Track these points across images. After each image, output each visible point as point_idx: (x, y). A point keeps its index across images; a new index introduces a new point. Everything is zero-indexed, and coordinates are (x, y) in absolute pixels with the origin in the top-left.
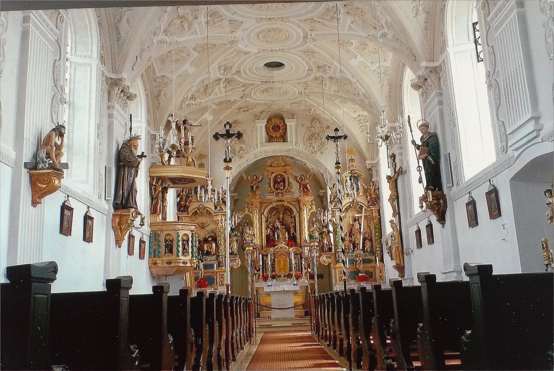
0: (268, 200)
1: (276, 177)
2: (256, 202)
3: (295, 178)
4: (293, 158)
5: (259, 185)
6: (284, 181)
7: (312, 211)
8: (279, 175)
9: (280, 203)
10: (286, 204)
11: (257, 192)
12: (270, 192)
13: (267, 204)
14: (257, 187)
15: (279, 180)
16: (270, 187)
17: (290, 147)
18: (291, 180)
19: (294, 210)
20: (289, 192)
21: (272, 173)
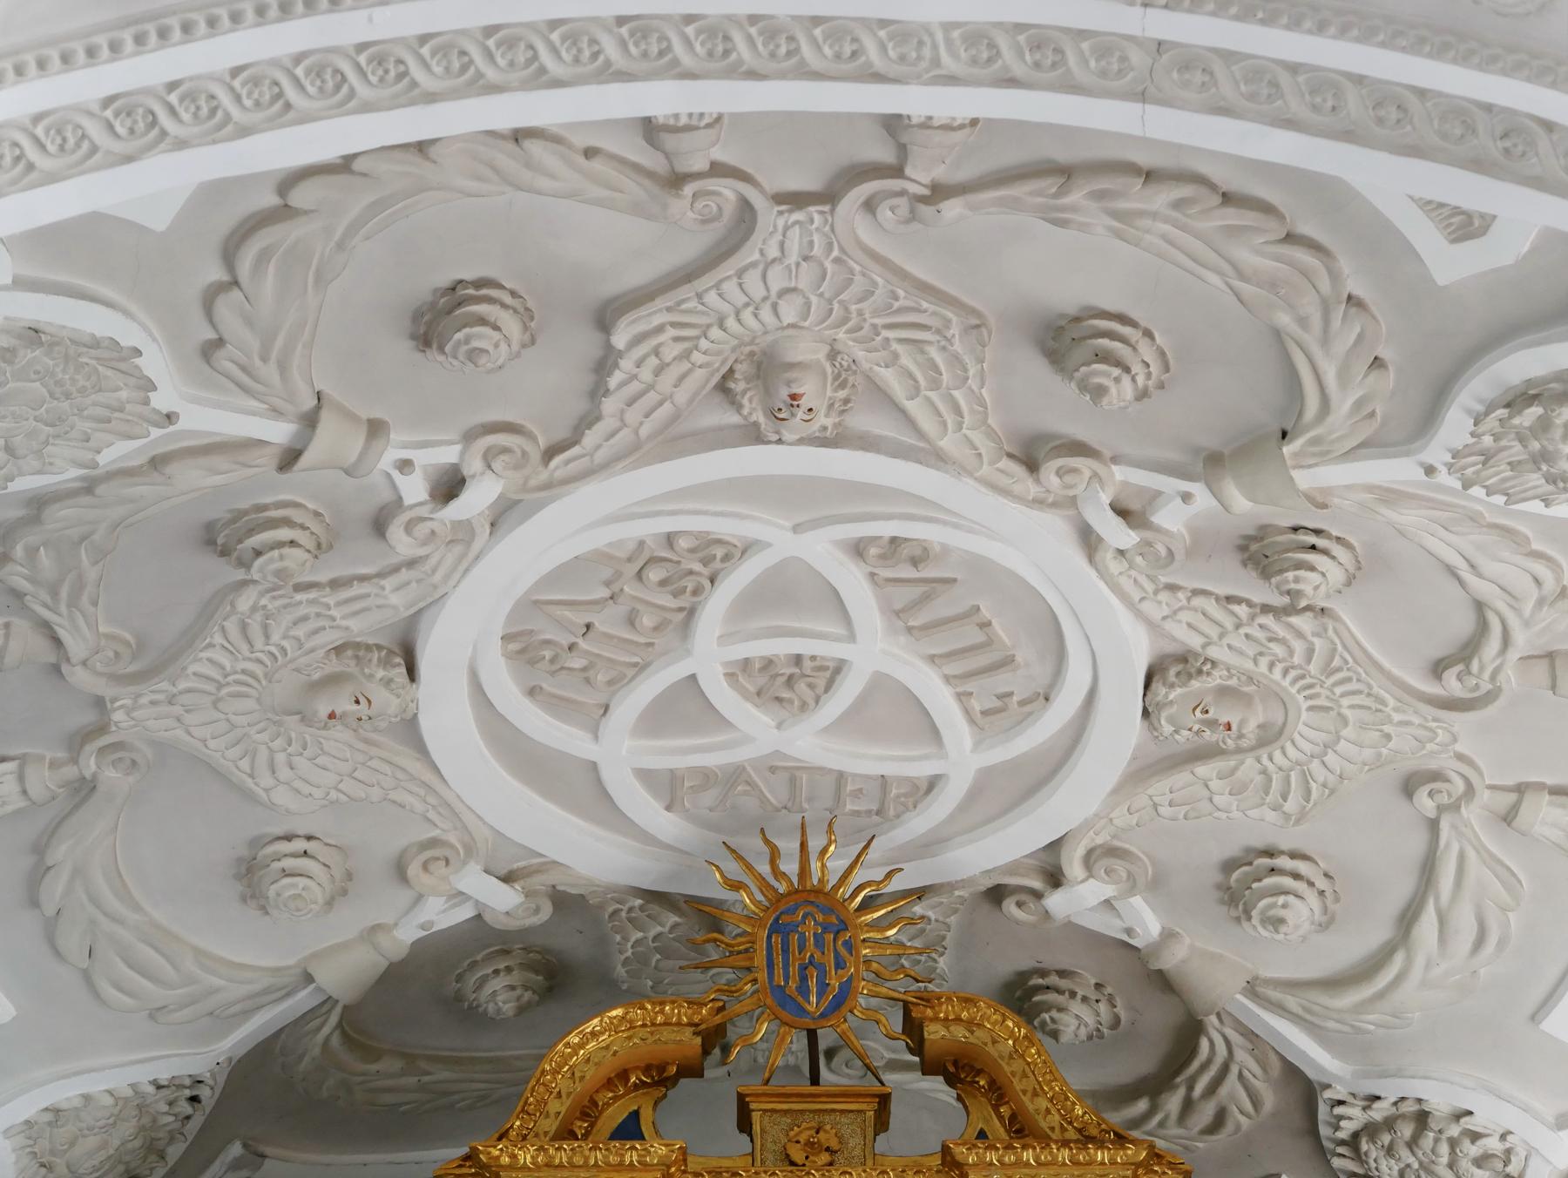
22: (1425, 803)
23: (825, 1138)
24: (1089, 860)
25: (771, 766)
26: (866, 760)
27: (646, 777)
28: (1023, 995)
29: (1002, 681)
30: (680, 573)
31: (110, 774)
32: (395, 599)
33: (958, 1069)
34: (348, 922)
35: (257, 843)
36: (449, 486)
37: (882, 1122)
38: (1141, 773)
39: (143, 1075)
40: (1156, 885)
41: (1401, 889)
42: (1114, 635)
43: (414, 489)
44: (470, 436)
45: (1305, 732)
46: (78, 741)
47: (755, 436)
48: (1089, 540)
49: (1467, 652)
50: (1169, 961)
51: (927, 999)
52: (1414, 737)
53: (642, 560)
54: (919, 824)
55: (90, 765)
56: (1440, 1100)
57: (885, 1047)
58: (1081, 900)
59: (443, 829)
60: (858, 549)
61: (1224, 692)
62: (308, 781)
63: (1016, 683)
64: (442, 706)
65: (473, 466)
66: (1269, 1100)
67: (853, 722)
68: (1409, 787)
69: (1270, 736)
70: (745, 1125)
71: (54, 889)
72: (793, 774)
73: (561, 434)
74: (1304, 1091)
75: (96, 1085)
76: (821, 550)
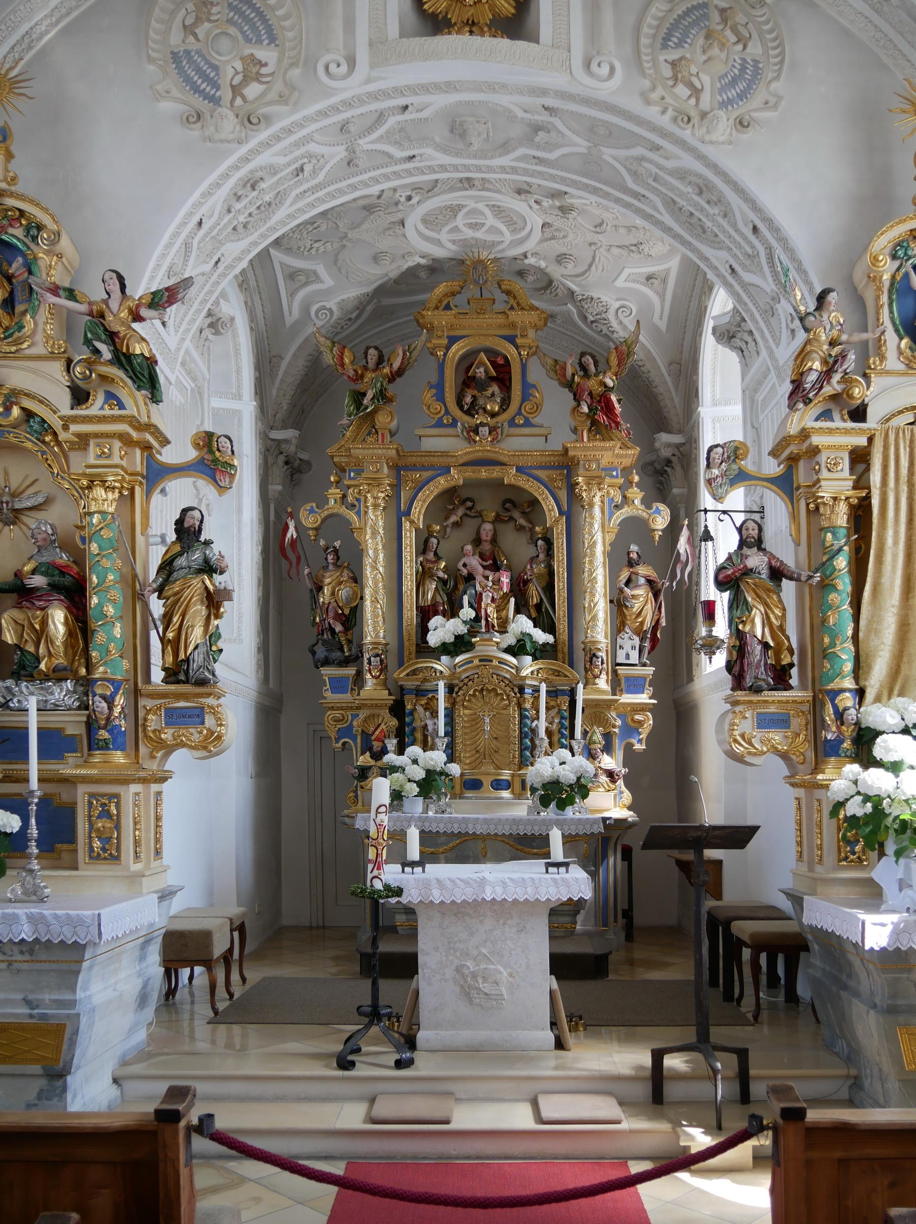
0: (430, 454)
1: (467, 362)
2: (376, 455)
3: (557, 369)
4: (547, 284)
5: (391, 390)
6: (502, 374)
7: (625, 512)
8: (489, 352)
9: (484, 473)
10: (510, 476)
11: (382, 419)
12: (439, 424)
13: (427, 474)
14: (382, 396)
15: (480, 372)
16: (440, 397)
17: (557, 80)
18: (537, 373)
19: (549, 505)
20: (528, 424)
22: (593, 247)
25: (472, 238)
26: (490, 238)
27: (449, 241)
28: (521, 273)
29: (515, 226)
30: (454, 210)
31: (348, 244)
32: (400, 216)
34: (394, 266)
35: (377, 254)
36: (409, 198)
38: (541, 241)
39: (358, 293)
40: (545, 259)
41: (589, 260)
42: (535, 220)
43: (403, 199)
44: (413, 190)
45: (571, 236)
46: (342, 239)
47: (467, 189)
48: (531, 208)
49: (601, 225)
50: (548, 270)
51: (502, 281)
52: (591, 237)
53: (446, 208)
55: (344, 242)
56: (595, 296)
58: (531, 261)
59: (411, 250)
60: (487, 206)
61: (556, 230)
62: (386, 243)
63: (518, 226)
64: (410, 230)
65: (413, 195)
66: (565, 292)
67: (488, 231)
68: (590, 244)
69: (564, 237)
70: (469, 303)
71: (339, 263)
72: (476, 239)
73: (430, 188)
74: (572, 293)
75: (350, 295)
76: (481, 206)
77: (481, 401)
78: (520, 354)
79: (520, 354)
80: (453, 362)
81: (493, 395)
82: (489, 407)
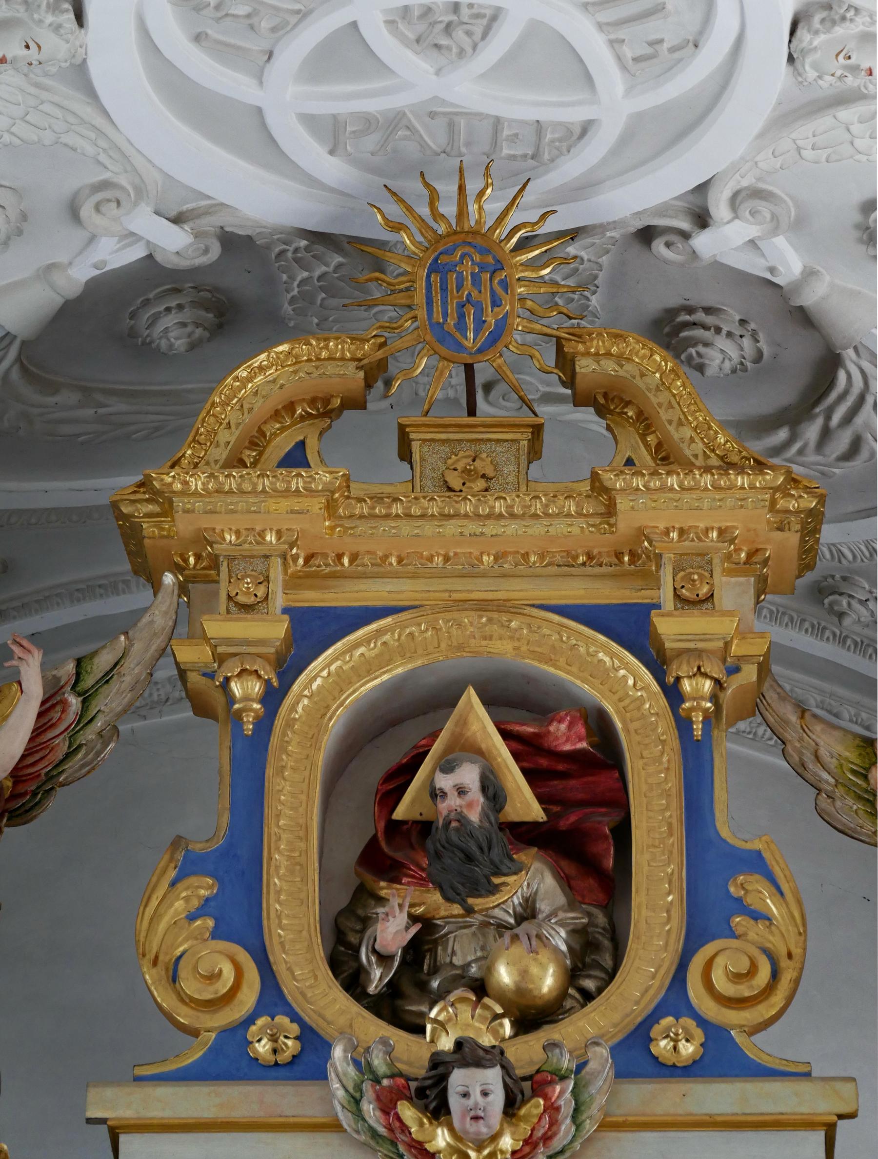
1: (393, 739)
21: (315, 630)
23: (483, 466)
24: (734, 201)
26: (521, 106)
27: (310, 121)
29: (653, 28)
33: (608, 402)
37: (535, 452)
38: (787, 117)
50: (809, 298)
51: (578, 336)
54: (572, 168)
57: (541, 381)
58: (726, 241)
59: (114, 172)
67: (509, 67)
70: (405, 454)
72: (451, 120)
77: (461, 950)
78: (673, 694)
79: (673, 694)
80: (314, 740)
81: (528, 913)
82: (504, 975)
